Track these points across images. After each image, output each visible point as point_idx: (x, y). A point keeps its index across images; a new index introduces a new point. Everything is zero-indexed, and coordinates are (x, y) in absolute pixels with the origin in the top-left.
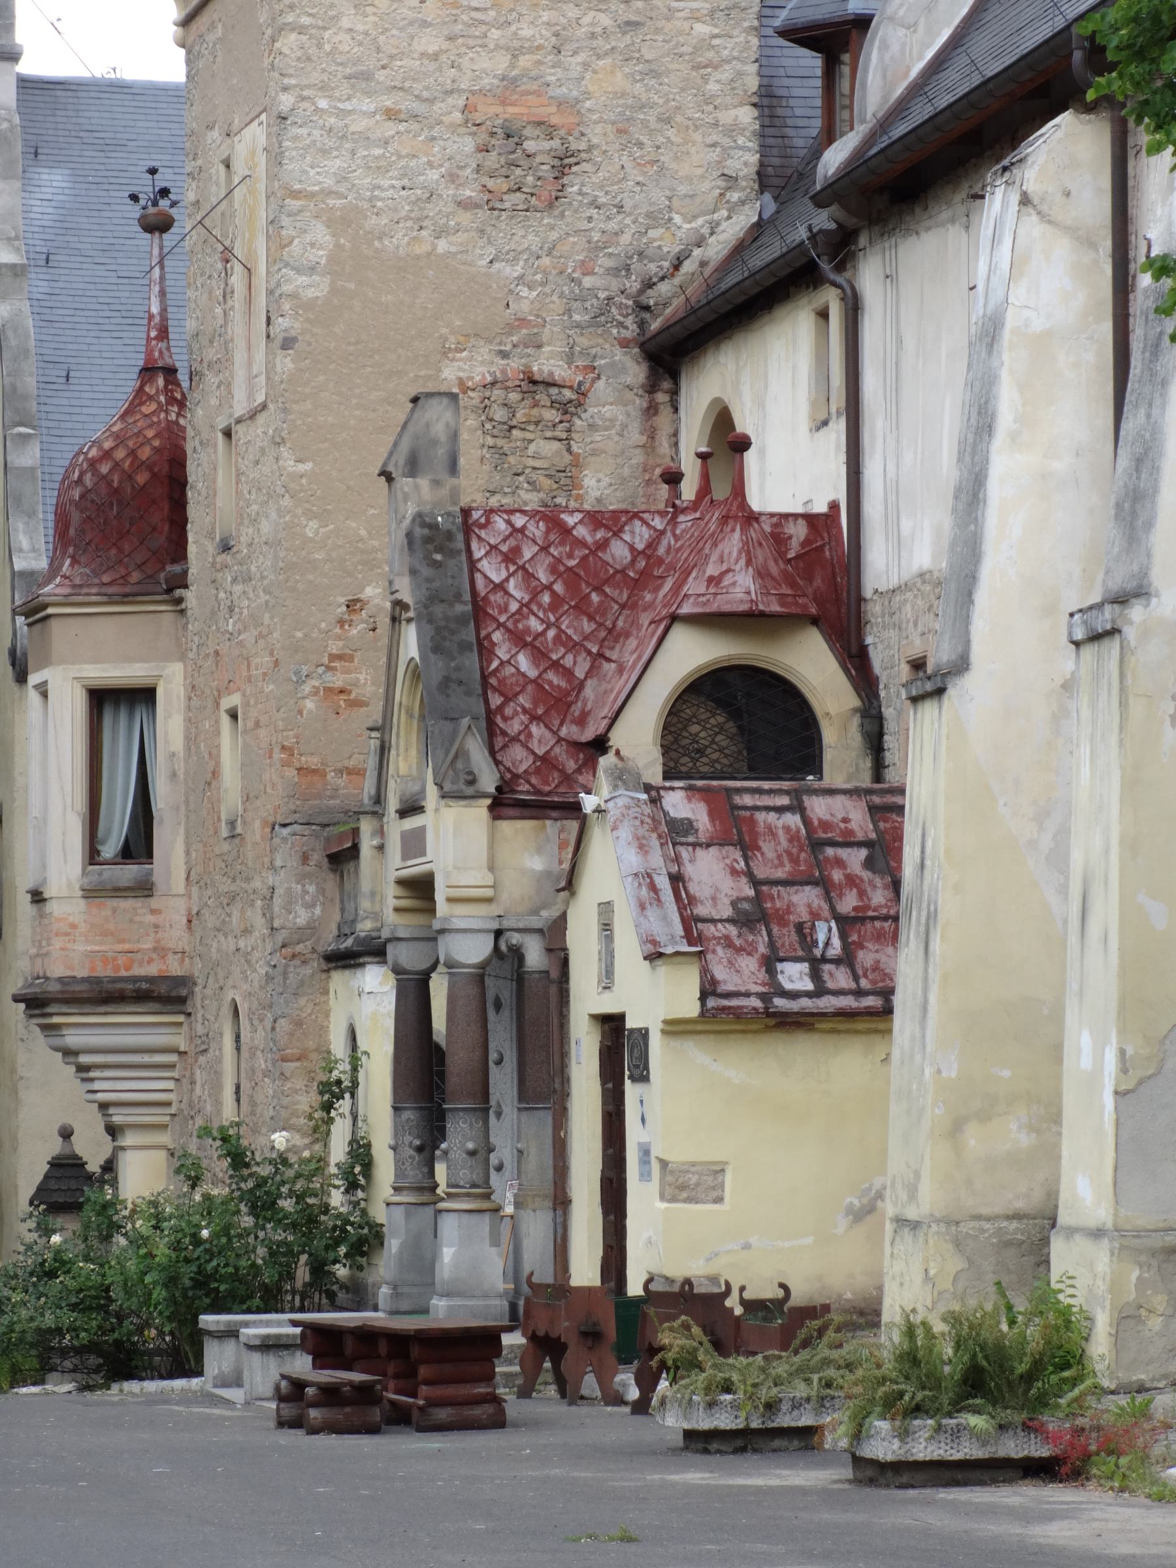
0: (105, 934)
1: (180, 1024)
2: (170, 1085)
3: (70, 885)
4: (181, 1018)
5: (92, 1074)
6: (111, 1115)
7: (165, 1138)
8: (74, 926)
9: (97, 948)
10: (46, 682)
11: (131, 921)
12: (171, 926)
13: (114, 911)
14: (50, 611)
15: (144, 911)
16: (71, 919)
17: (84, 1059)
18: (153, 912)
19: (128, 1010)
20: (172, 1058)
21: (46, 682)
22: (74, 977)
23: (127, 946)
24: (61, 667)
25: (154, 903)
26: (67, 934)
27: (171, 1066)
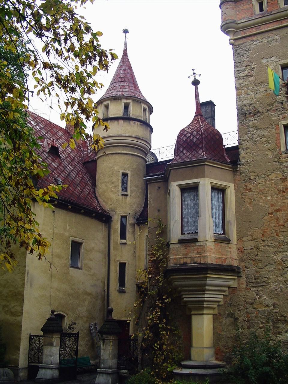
0: (219, 252)
1: (235, 279)
2: (222, 296)
3: (211, 238)
4: (236, 278)
5: (206, 292)
6: (204, 304)
7: (211, 312)
8: (212, 249)
9: (218, 256)
10: (200, 182)
11: (225, 250)
12: (233, 252)
13: (221, 246)
14: (206, 163)
15: (228, 247)
16: (211, 247)
17: (207, 288)
18: (230, 248)
19: (228, 274)
20: (227, 289)
21: (200, 182)
22: (213, 264)
23: (224, 257)
24: (208, 178)
25: (230, 245)
26: (210, 251)
27: (225, 291)
